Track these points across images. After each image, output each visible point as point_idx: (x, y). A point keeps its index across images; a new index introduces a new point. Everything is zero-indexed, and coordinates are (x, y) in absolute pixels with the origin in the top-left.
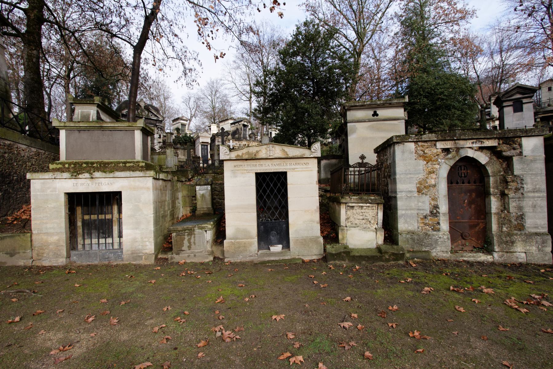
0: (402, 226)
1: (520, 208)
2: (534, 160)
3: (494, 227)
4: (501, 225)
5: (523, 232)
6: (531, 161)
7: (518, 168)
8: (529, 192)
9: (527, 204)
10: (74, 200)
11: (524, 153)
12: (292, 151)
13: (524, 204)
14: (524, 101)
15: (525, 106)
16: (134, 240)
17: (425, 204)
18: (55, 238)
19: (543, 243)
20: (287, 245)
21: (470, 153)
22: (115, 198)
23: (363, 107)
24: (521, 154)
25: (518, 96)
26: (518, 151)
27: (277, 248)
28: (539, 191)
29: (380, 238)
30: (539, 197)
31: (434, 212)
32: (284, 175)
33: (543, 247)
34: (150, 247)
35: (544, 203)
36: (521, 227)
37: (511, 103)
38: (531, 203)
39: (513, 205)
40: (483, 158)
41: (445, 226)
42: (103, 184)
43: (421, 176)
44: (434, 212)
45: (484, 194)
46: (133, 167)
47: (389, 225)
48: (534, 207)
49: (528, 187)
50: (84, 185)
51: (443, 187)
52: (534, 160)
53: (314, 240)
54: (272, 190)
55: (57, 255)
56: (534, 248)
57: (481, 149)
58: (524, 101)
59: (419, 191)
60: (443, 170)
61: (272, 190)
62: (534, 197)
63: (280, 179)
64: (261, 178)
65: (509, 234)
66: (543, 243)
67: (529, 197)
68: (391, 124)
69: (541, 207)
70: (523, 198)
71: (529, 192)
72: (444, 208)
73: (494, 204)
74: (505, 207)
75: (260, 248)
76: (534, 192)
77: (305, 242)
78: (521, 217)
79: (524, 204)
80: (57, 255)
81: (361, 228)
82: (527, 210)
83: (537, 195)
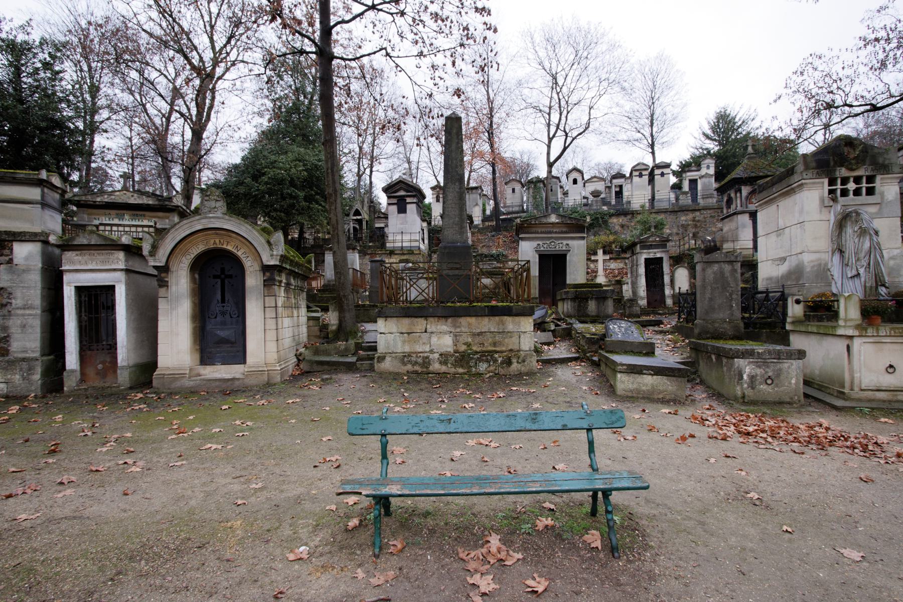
2: (27, 270)
5: (7, 358)
6: (24, 271)
8: (18, 308)
11: (15, 261)
13: (10, 323)
14: (408, 200)
15: (409, 207)
19: (30, 369)
24: (10, 261)
25: (402, 193)
26: (7, 258)
28: (31, 307)
30: (31, 315)
33: (29, 375)
37: (395, 201)
38: (19, 322)
48: (24, 326)
49: (17, 302)
52: (27, 270)
56: (18, 377)
58: (408, 200)
62: (23, 315)
66: (30, 369)
67: (18, 315)
68: (17, 208)
69: (32, 327)
70: (10, 315)
71: (18, 308)
76: (24, 309)
79: (10, 323)
83: (27, 312)
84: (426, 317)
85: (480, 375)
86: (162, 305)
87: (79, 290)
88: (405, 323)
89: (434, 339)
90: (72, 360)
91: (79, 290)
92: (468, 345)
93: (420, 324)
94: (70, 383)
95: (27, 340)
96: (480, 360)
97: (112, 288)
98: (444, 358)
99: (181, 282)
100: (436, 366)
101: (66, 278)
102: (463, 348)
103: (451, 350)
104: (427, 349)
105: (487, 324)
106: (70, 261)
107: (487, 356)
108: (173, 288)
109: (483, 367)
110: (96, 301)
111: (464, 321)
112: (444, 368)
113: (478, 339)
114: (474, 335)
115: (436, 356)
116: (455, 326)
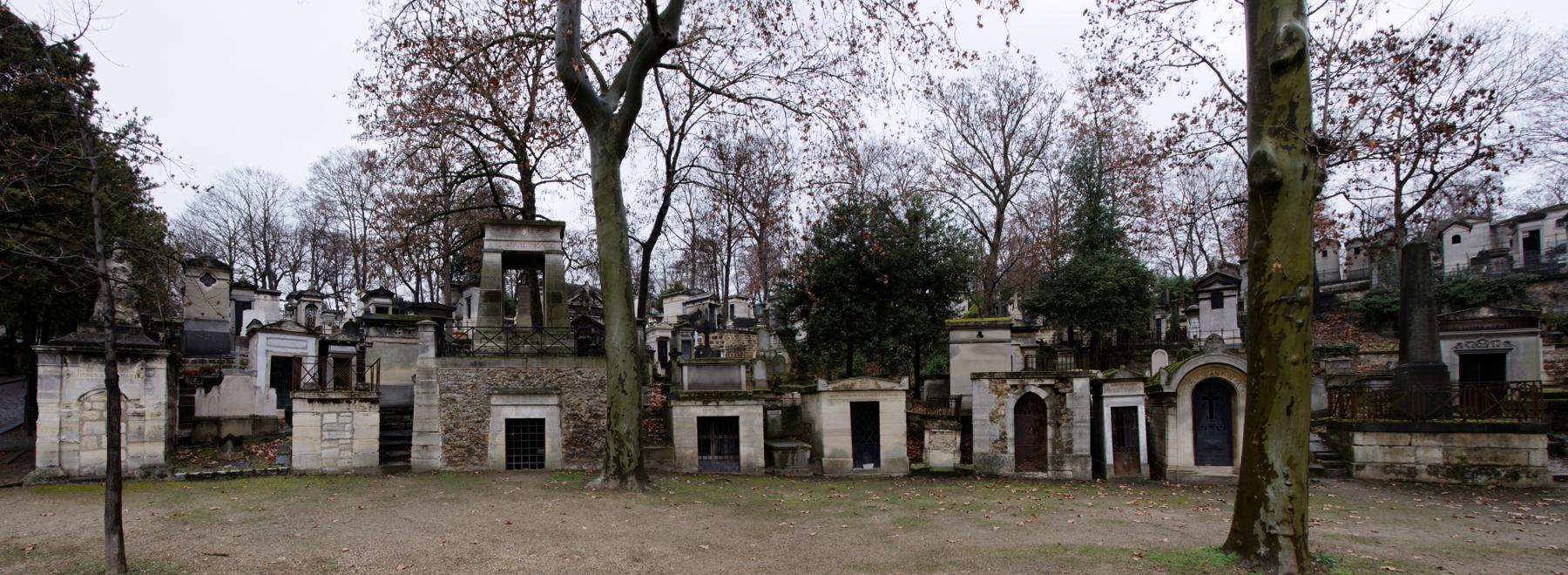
0: (976, 449)
1: (1070, 435)
3: (1050, 450)
4: (1054, 449)
7: (1069, 403)
9: (1075, 432)
10: (703, 422)
12: (884, 384)
16: (749, 456)
17: (995, 431)
18: (690, 452)
20: (877, 464)
21: (1033, 390)
22: (734, 421)
23: (966, 327)
27: (870, 466)
29: (958, 459)
31: (1003, 437)
32: (877, 404)
34: (761, 461)
35: (1088, 432)
36: (1070, 451)
39: (1064, 433)
40: (1043, 394)
41: (1011, 449)
42: (727, 411)
43: (993, 407)
44: (1003, 437)
45: (1044, 424)
46: (746, 397)
47: (966, 450)
49: (1076, 418)
50: (711, 411)
51: (1010, 417)
53: (902, 460)
54: (865, 419)
55: (692, 465)
57: (1042, 386)
59: (992, 420)
60: (1011, 401)
61: (865, 419)
63: (874, 407)
64: (855, 406)
65: (1061, 457)
72: (1011, 434)
73: (1050, 432)
74: (1057, 435)
75: (855, 465)
77: (892, 462)
78: (1070, 443)
80: (692, 465)
81: (942, 451)
82: (1075, 437)
84: (1410, 432)
85: (1479, 487)
86: (1171, 420)
87: (1113, 409)
88: (1386, 438)
89: (1420, 453)
90: (1109, 458)
91: (1113, 409)
92: (1463, 459)
93: (1404, 439)
94: (1110, 473)
95: (1082, 445)
96: (1478, 473)
97: (1135, 408)
98: (1433, 469)
99: (1185, 404)
100: (1425, 476)
101: (1105, 401)
102: (1456, 461)
103: (1441, 462)
104: (1412, 460)
105: (1484, 440)
106: (1108, 390)
107: (1484, 469)
108: (1180, 408)
109: (1481, 479)
110: (1124, 417)
111: (1457, 438)
112: (1433, 478)
113: (1474, 454)
114: (1469, 450)
115: (1424, 467)
116: (1445, 441)
